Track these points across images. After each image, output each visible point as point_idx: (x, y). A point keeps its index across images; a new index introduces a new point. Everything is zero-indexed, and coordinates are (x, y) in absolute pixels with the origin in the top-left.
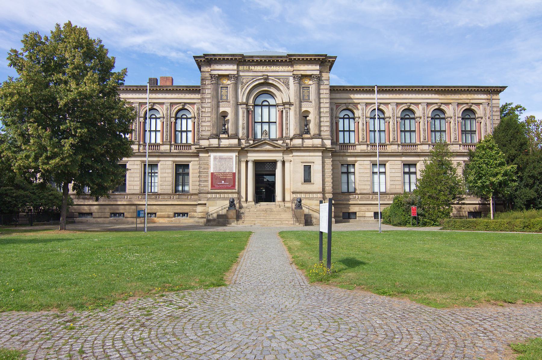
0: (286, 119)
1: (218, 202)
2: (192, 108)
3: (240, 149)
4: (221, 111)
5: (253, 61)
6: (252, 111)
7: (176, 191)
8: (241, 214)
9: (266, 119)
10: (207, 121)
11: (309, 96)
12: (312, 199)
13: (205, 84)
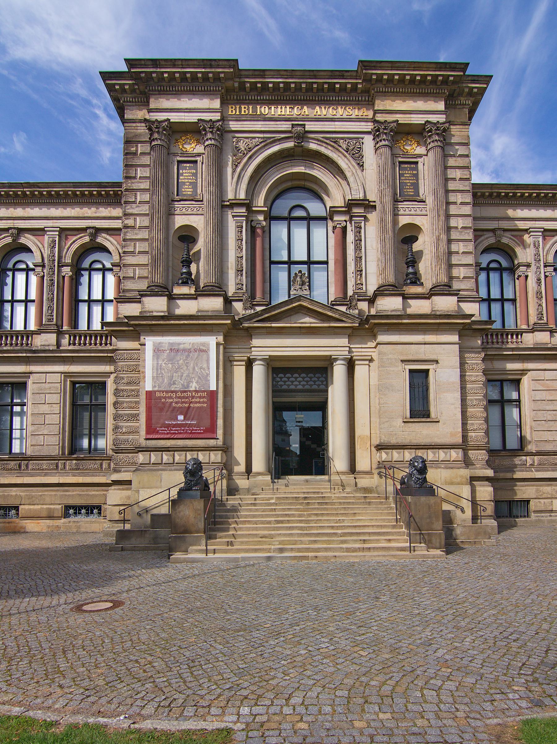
2: (115, 243)
4: (177, 226)
6: (263, 227)
7: (74, 449)
8: (229, 511)
9: (300, 254)
10: (140, 252)
11: (416, 186)
13: (135, 154)
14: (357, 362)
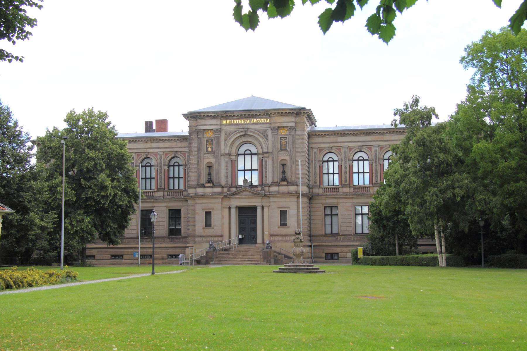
1: (203, 244)
9: (248, 167)
11: (286, 146)
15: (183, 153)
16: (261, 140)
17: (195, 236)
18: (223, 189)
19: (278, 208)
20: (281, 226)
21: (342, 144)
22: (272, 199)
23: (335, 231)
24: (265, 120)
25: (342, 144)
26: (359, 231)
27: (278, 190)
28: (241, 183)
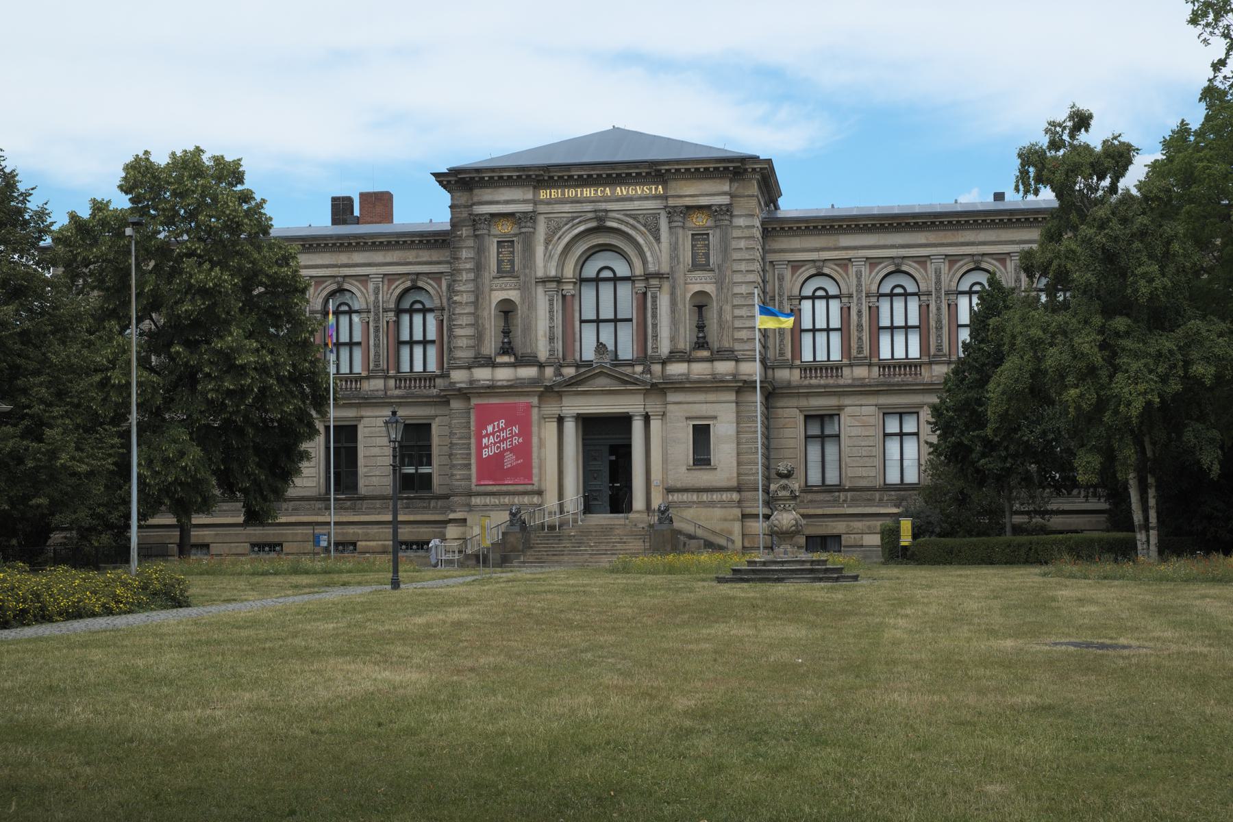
0: (653, 312)
1: (492, 514)
3: (542, 389)
5: (571, 177)
11: (707, 256)
12: (712, 504)
14: (652, 417)
15: (437, 277)
16: (640, 240)
17: (470, 494)
18: (542, 369)
19: (687, 418)
20: (694, 464)
21: (850, 254)
22: (672, 397)
23: (832, 478)
24: (650, 189)
25: (850, 254)
26: (893, 477)
27: (686, 371)
28: (589, 354)
